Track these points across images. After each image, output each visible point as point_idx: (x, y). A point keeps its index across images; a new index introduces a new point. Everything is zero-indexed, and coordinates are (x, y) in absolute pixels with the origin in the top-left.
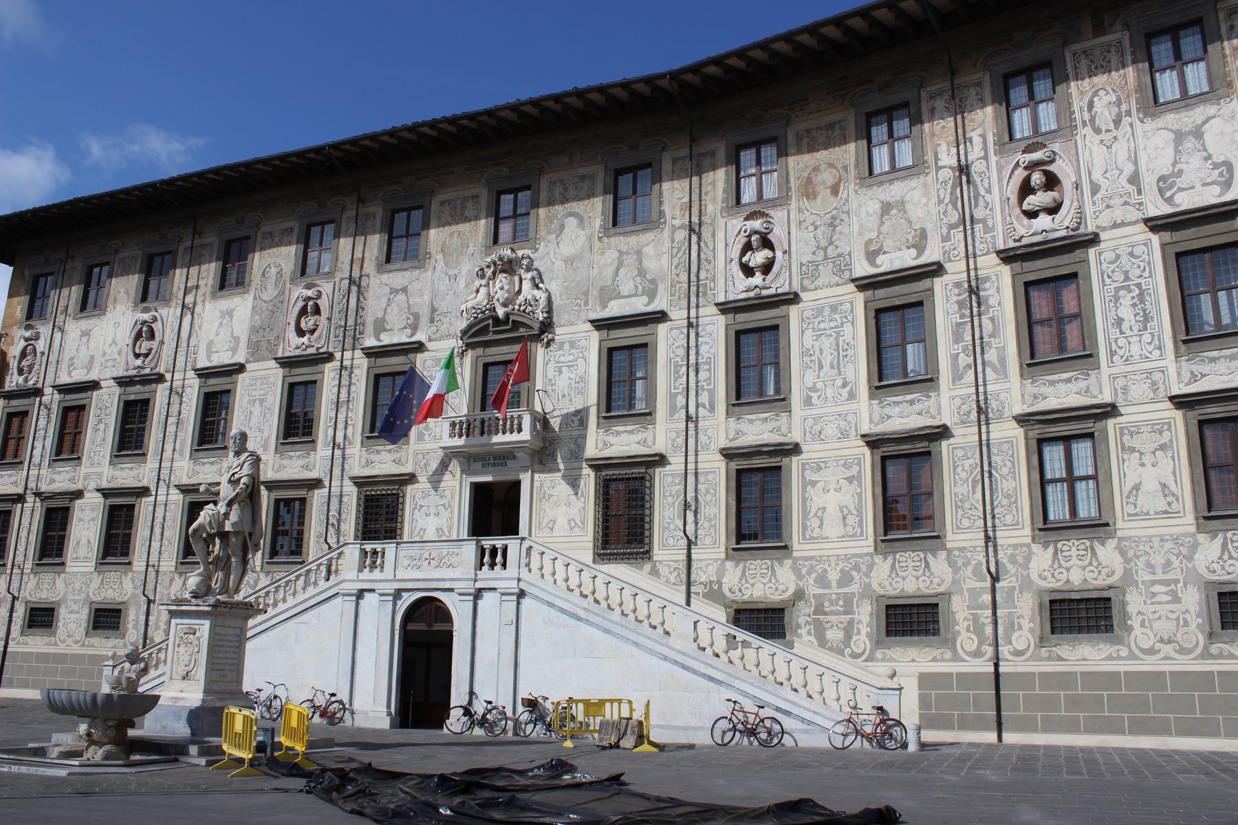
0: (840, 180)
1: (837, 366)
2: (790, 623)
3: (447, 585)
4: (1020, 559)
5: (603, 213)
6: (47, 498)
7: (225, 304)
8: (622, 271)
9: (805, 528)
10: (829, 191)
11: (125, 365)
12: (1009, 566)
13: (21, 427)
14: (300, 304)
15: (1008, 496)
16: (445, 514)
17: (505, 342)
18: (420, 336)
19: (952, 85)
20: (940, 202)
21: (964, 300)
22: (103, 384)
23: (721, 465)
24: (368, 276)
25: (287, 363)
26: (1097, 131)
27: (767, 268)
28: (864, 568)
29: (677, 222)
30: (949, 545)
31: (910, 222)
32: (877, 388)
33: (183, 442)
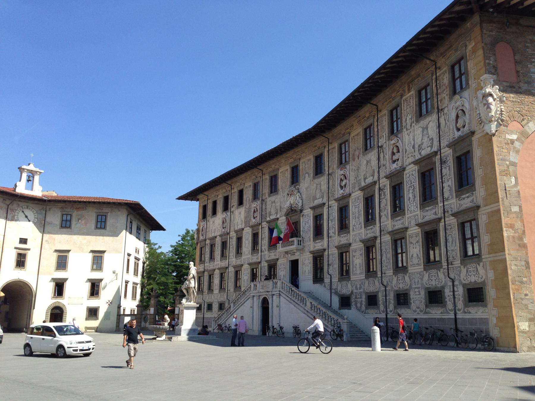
7: (239, 210)
18: (278, 216)
26: (407, 130)
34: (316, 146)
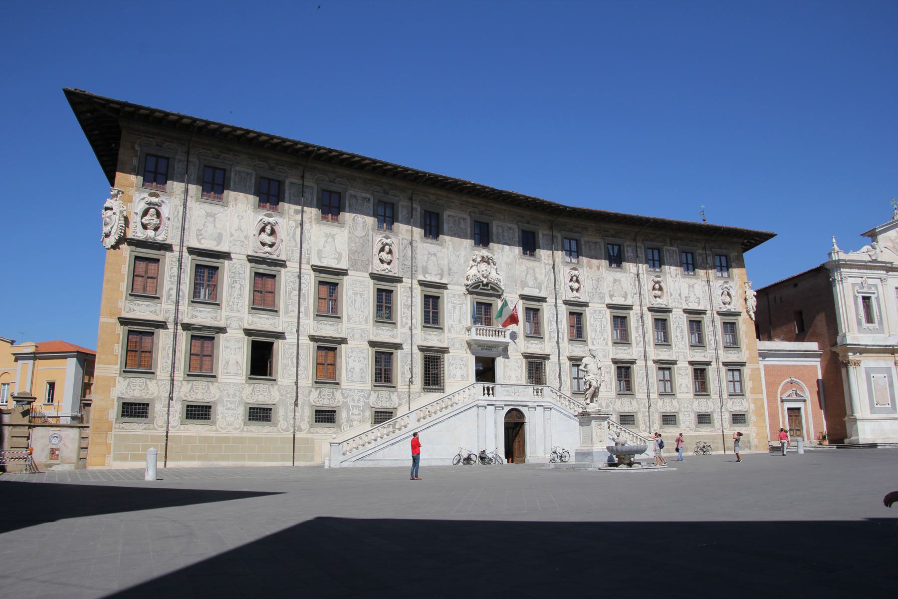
11: (253, 248)
27: (577, 290)
33: (307, 308)
34: (523, 217)
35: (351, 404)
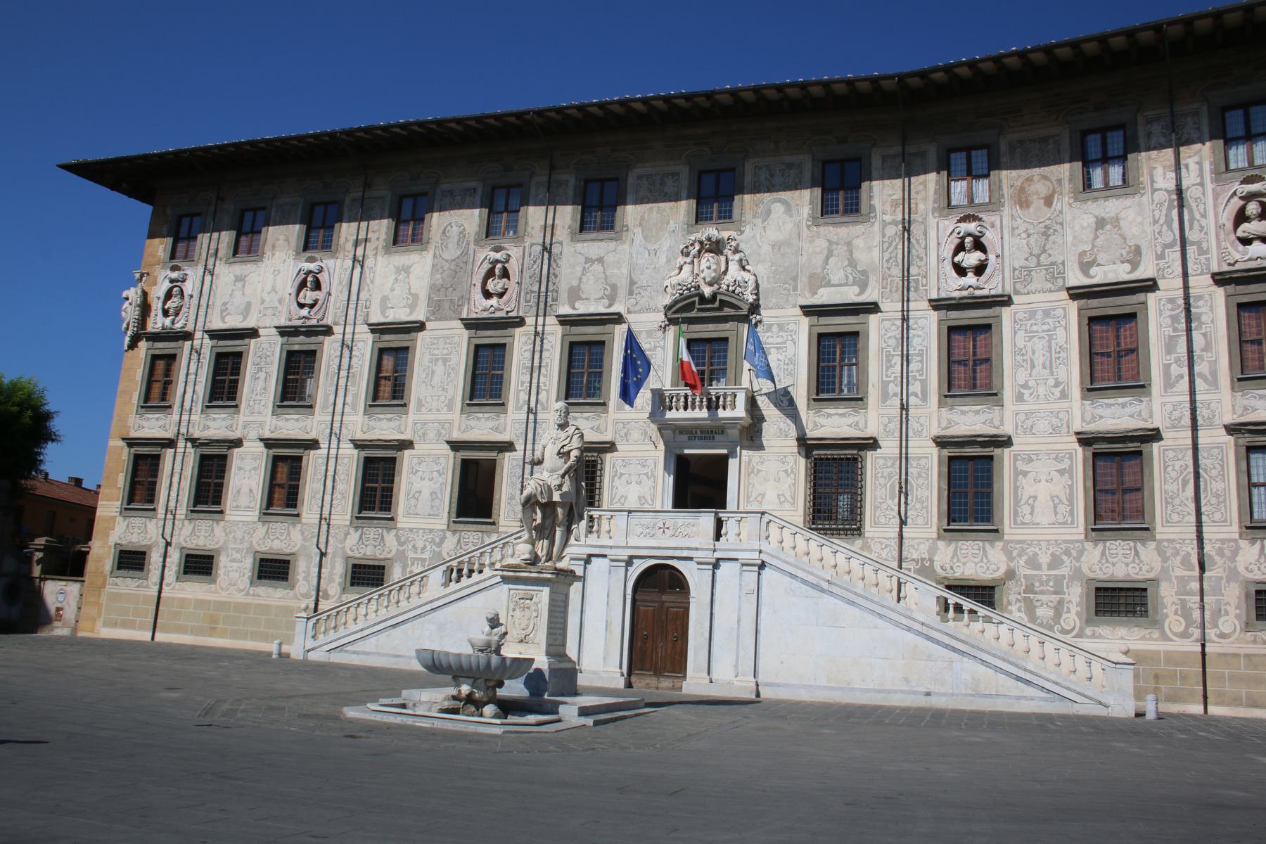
0: (1054, 192)
1: (1050, 366)
2: (1001, 600)
3: (685, 554)
4: (1227, 553)
5: (811, 203)
6: (202, 444)
8: (832, 260)
9: (1016, 514)
10: (1042, 201)
11: (288, 314)
12: (1217, 558)
13: (168, 372)
14: (487, 266)
15: (1217, 496)
16: (648, 483)
17: (713, 323)
19: (1172, 111)
20: (1155, 222)
21: (1178, 315)
22: (261, 332)
23: (934, 451)
24: (561, 243)
25: (473, 325)
27: (980, 269)
28: (1074, 553)
29: (888, 218)
30: (1158, 537)
31: (1125, 239)
32: (1089, 390)
33: (356, 396)
35: (411, 555)
